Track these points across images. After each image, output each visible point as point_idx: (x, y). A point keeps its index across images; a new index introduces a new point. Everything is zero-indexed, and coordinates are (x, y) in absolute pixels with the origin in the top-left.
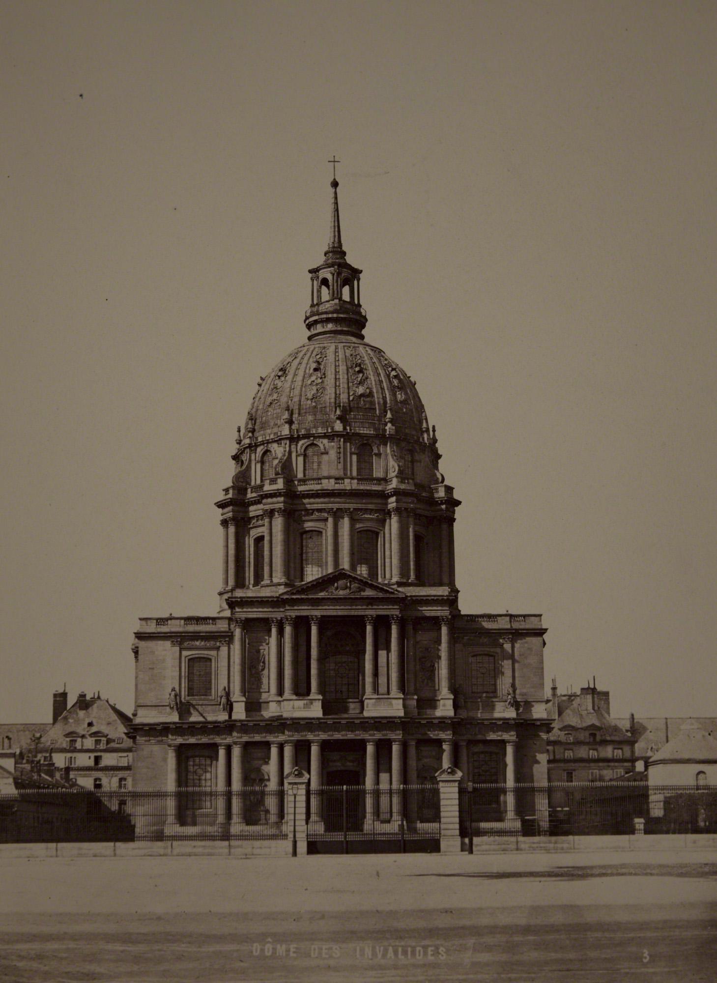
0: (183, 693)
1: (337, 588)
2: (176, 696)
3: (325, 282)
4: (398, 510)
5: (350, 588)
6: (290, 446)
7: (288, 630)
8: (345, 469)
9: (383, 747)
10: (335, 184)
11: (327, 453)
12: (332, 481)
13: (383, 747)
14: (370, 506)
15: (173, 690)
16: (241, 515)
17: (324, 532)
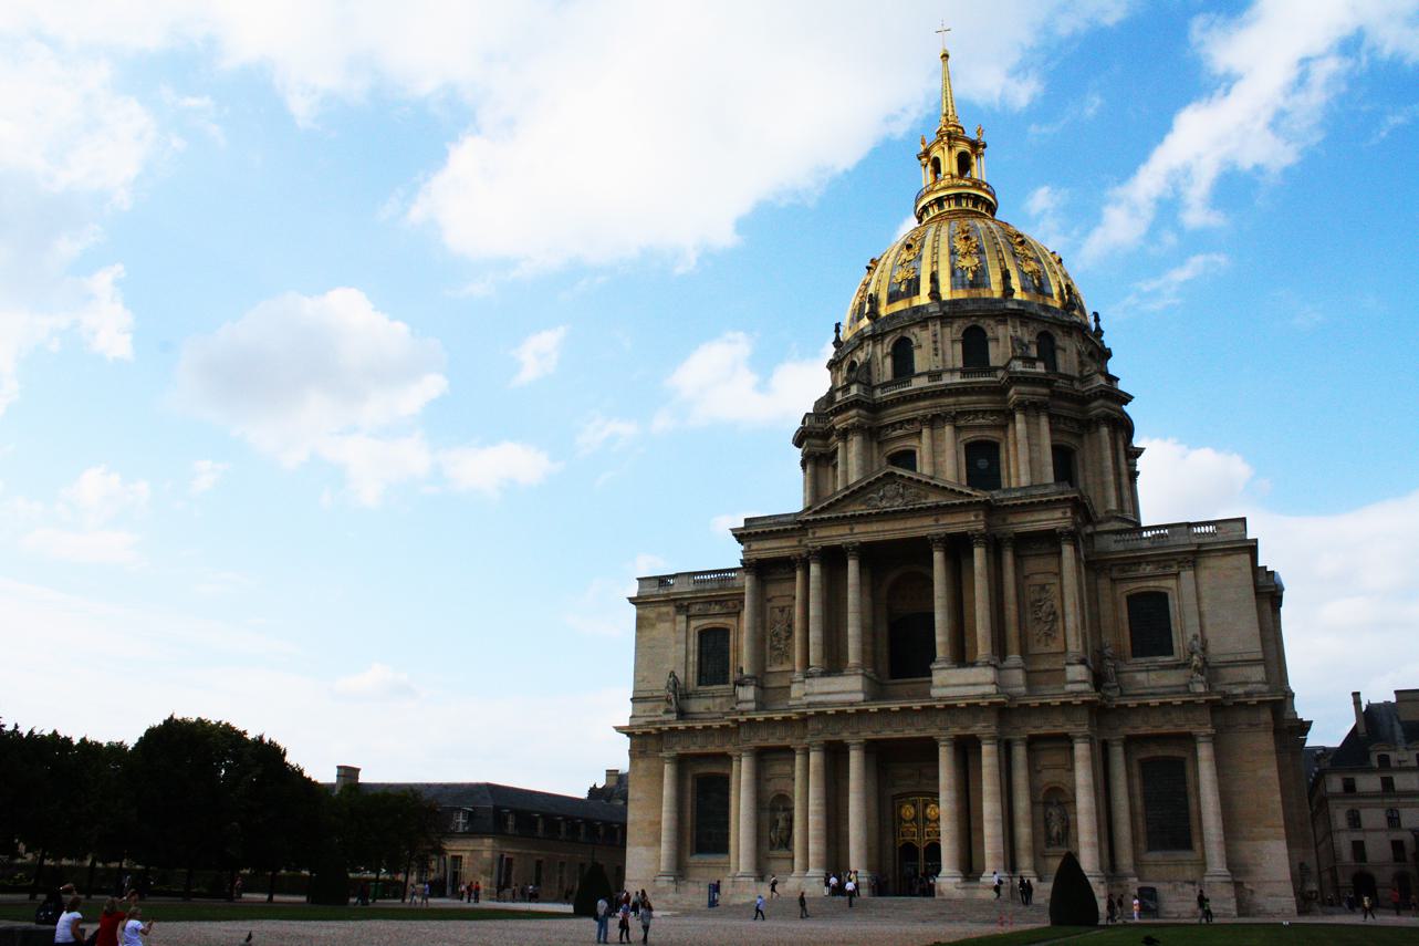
0: (691, 681)
1: (881, 499)
2: (675, 685)
3: (936, 163)
4: (1024, 406)
5: (902, 496)
6: (874, 346)
7: (814, 569)
8: (944, 361)
9: (967, 750)
10: (946, 56)
11: (920, 346)
12: (926, 379)
13: (967, 750)
14: (979, 407)
15: (672, 674)
16: (822, 450)
17: (918, 451)
